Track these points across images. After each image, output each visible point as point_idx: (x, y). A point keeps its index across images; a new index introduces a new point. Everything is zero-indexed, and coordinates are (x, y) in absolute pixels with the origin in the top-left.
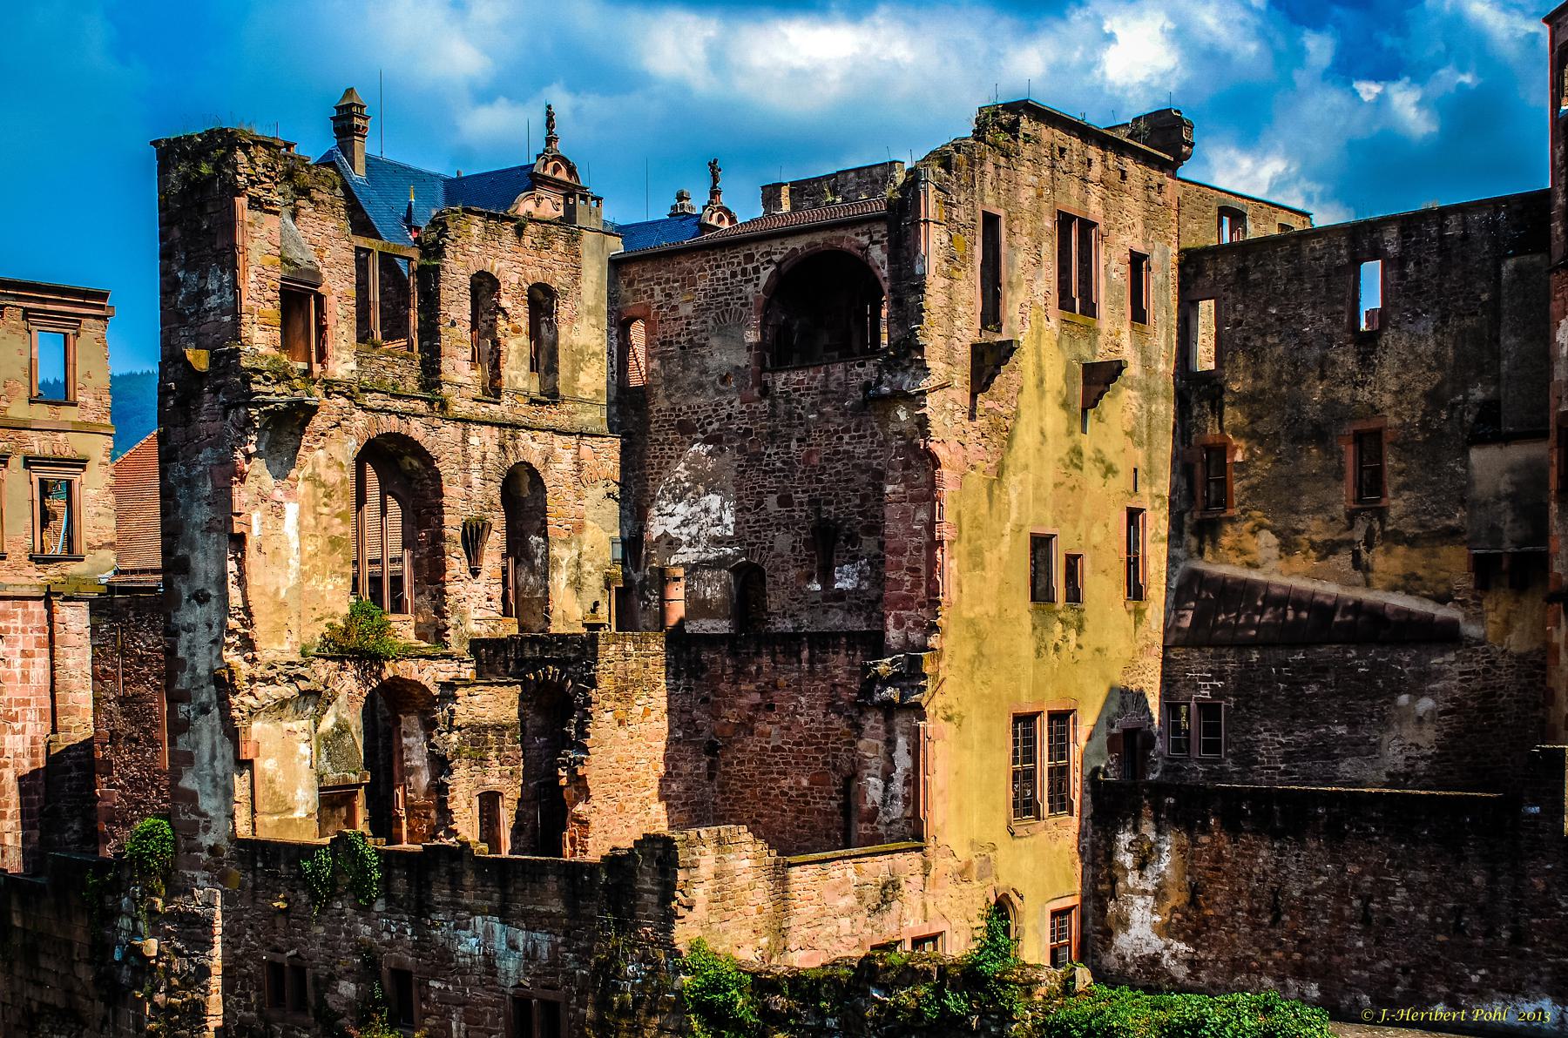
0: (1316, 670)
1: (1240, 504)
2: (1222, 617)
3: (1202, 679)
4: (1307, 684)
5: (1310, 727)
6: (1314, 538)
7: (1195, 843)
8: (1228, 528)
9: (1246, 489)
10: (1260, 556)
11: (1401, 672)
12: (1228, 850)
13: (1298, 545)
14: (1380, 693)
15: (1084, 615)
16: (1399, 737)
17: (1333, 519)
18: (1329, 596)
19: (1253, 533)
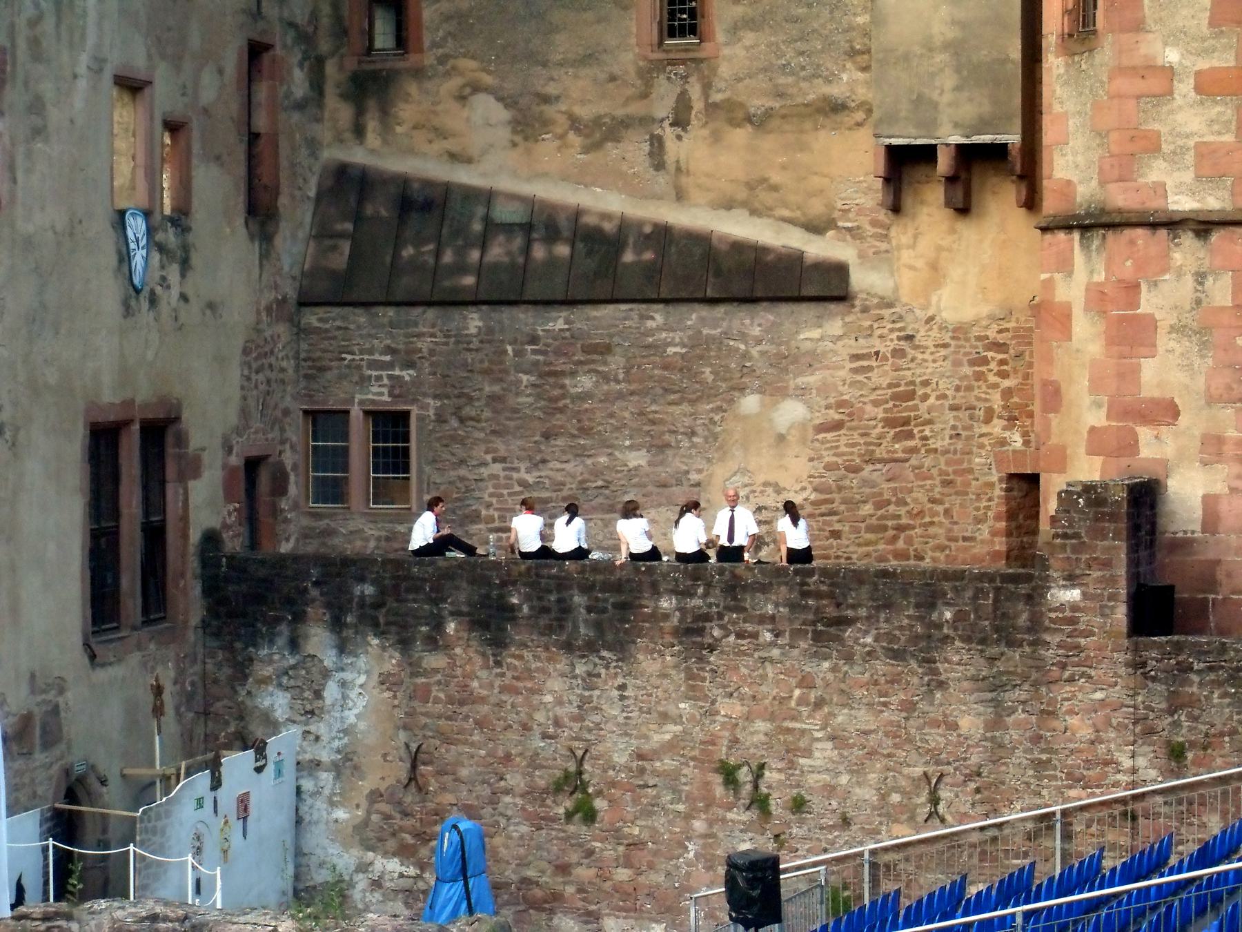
0: (588, 350)
1: (435, 45)
2: (408, 252)
3: (374, 365)
4: (573, 374)
5: (581, 453)
6: (579, 111)
7: (415, 669)
8: (412, 88)
9: (448, 18)
10: (474, 142)
11: (746, 356)
12: (482, 679)
13: (546, 123)
14: (708, 393)
15: (191, 238)
16: (744, 471)
17: (613, 78)
18: (606, 216)
19: (462, 98)
